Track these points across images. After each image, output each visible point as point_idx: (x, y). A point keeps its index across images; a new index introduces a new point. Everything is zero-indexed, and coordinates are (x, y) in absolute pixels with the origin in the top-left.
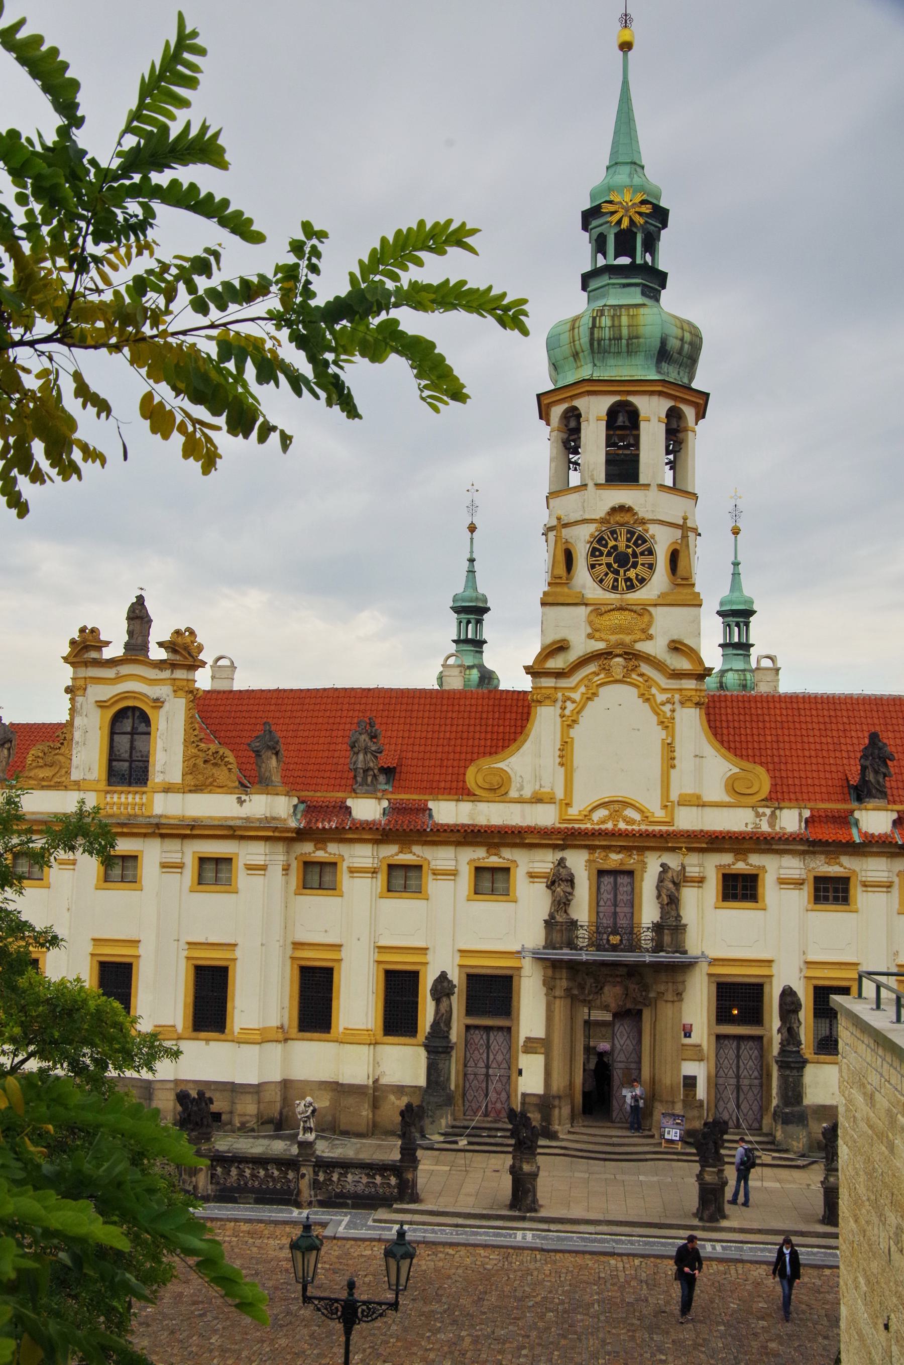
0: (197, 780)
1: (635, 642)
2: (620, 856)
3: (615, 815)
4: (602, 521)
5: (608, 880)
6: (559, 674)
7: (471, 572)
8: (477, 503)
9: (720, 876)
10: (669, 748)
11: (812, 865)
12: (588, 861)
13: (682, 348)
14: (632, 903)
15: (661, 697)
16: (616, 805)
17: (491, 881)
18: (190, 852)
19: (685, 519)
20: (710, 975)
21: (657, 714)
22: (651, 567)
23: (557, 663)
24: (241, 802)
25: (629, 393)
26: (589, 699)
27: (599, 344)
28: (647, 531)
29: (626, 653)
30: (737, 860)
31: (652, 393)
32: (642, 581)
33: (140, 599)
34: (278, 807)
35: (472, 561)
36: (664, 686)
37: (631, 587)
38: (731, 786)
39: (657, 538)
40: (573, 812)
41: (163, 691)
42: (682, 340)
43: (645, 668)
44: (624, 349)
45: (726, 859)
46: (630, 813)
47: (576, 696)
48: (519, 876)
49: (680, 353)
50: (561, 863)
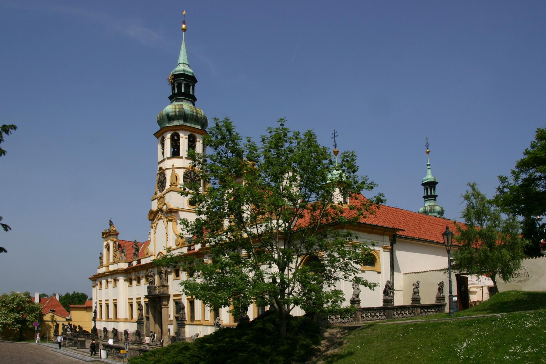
13: (175, 115)
42: (175, 112)
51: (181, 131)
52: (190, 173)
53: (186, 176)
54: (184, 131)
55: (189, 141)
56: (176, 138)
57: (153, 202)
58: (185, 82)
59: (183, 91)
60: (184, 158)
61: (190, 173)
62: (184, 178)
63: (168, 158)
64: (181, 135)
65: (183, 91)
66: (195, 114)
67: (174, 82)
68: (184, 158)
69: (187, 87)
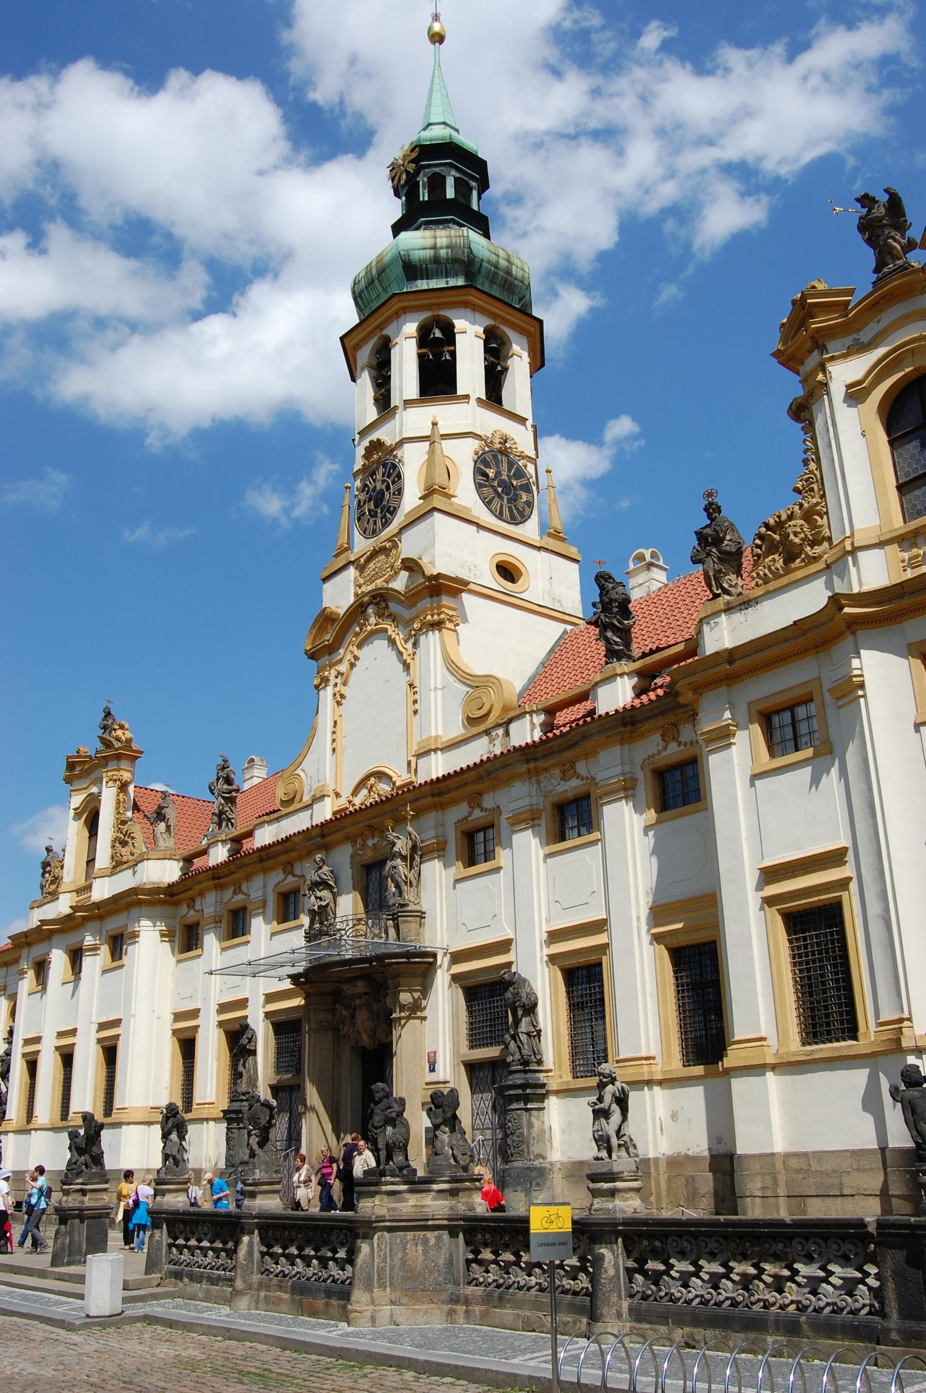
1: (387, 581)
2: (376, 840)
5: (375, 875)
9: (459, 834)
11: (550, 787)
12: (352, 856)
19: (435, 424)
20: (455, 978)
22: (400, 492)
23: (328, 637)
25: (381, 327)
26: (352, 665)
27: (361, 298)
28: (395, 456)
29: (374, 597)
30: (473, 808)
31: (397, 315)
32: (393, 512)
34: (167, 872)
36: (407, 618)
37: (386, 524)
39: (405, 460)
40: (342, 802)
42: (434, 247)
44: (380, 289)
45: (462, 810)
47: (343, 667)
49: (436, 260)
51: (461, 311)
52: (495, 457)
53: (482, 464)
54: (469, 312)
55: (487, 350)
56: (438, 334)
57: (327, 586)
58: (453, 172)
59: (450, 193)
60: (473, 401)
61: (495, 457)
62: (480, 472)
63: (408, 403)
64: (460, 324)
65: (450, 193)
66: (503, 263)
67: (417, 173)
68: (473, 401)
69: (462, 187)
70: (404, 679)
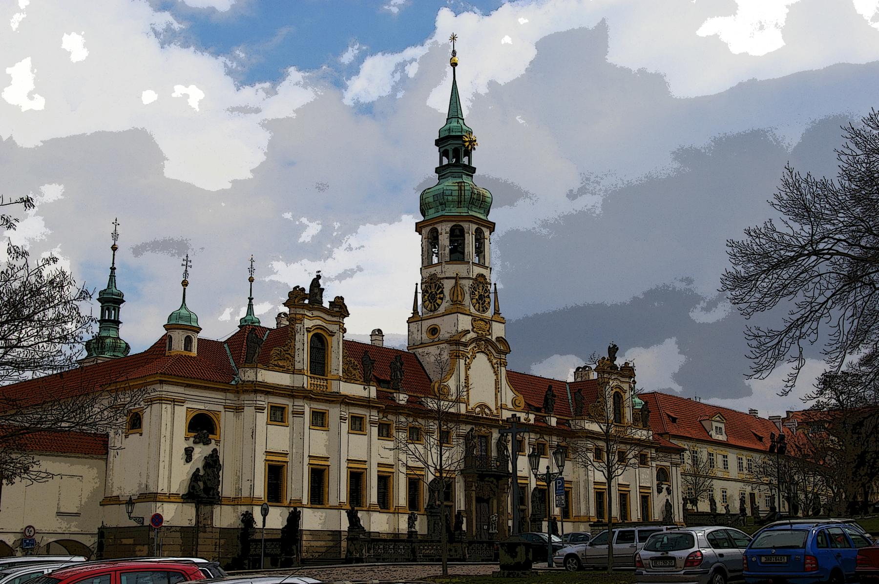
0: (348, 377)
3: (483, 411)
4: (476, 279)
6: (465, 345)
7: (112, 276)
8: (118, 232)
10: (497, 383)
14: (487, 449)
15: (494, 361)
16: (483, 406)
17: (444, 439)
18: (347, 412)
21: (493, 368)
24: (365, 389)
33: (319, 277)
35: (113, 269)
38: (514, 403)
41: (334, 328)
43: (490, 348)
46: (486, 410)
48: (454, 435)
50: (472, 430)
70: (495, 377)
